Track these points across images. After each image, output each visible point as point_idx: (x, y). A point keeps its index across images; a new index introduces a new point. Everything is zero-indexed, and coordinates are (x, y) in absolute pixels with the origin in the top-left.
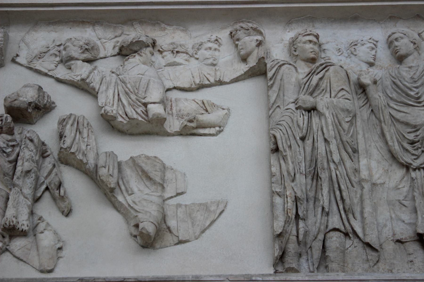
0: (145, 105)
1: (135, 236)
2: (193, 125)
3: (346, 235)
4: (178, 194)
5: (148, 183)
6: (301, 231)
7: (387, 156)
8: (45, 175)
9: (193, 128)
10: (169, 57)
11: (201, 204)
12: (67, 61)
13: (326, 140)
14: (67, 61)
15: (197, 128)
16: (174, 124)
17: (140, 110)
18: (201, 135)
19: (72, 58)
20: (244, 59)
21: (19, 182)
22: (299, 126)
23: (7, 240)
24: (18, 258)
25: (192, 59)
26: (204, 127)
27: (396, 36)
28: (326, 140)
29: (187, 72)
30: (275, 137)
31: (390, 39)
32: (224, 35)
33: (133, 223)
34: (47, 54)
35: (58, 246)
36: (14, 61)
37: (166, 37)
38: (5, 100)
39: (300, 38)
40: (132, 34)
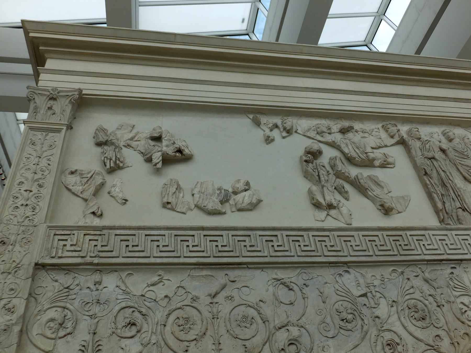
0: (366, 153)
1: (380, 210)
2: (385, 163)
3: (463, 210)
4: (389, 192)
5: (378, 187)
6: (447, 208)
7: (463, 179)
8: (333, 182)
9: (386, 164)
10: (361, 134)
11: (400, 197)
12: (321, 133)
13: (443, 171)
14: (321, 133)
15: (386, 164)
16: (377, 163)
17: (365, 155)
18: (389, 168)
19: (324, 132)
20: (392, 137)
21: (325, 184)
22: (428, 165)
23: (328, 210)
24: (335, 219)
25: (370, 136)
26: (388, 165)
27: (448, 131)
28: (443, 171)
29: (371, 141)
30: (424, 169)
31: (444, 132)
32: (380, 126)
33: (378, 204)
34: (311, 130)
35: (350, 213)
36: (296, 132)
37: (357, 126)
38: (306, 148)
39: (413, 129)
40: (346, 124)
